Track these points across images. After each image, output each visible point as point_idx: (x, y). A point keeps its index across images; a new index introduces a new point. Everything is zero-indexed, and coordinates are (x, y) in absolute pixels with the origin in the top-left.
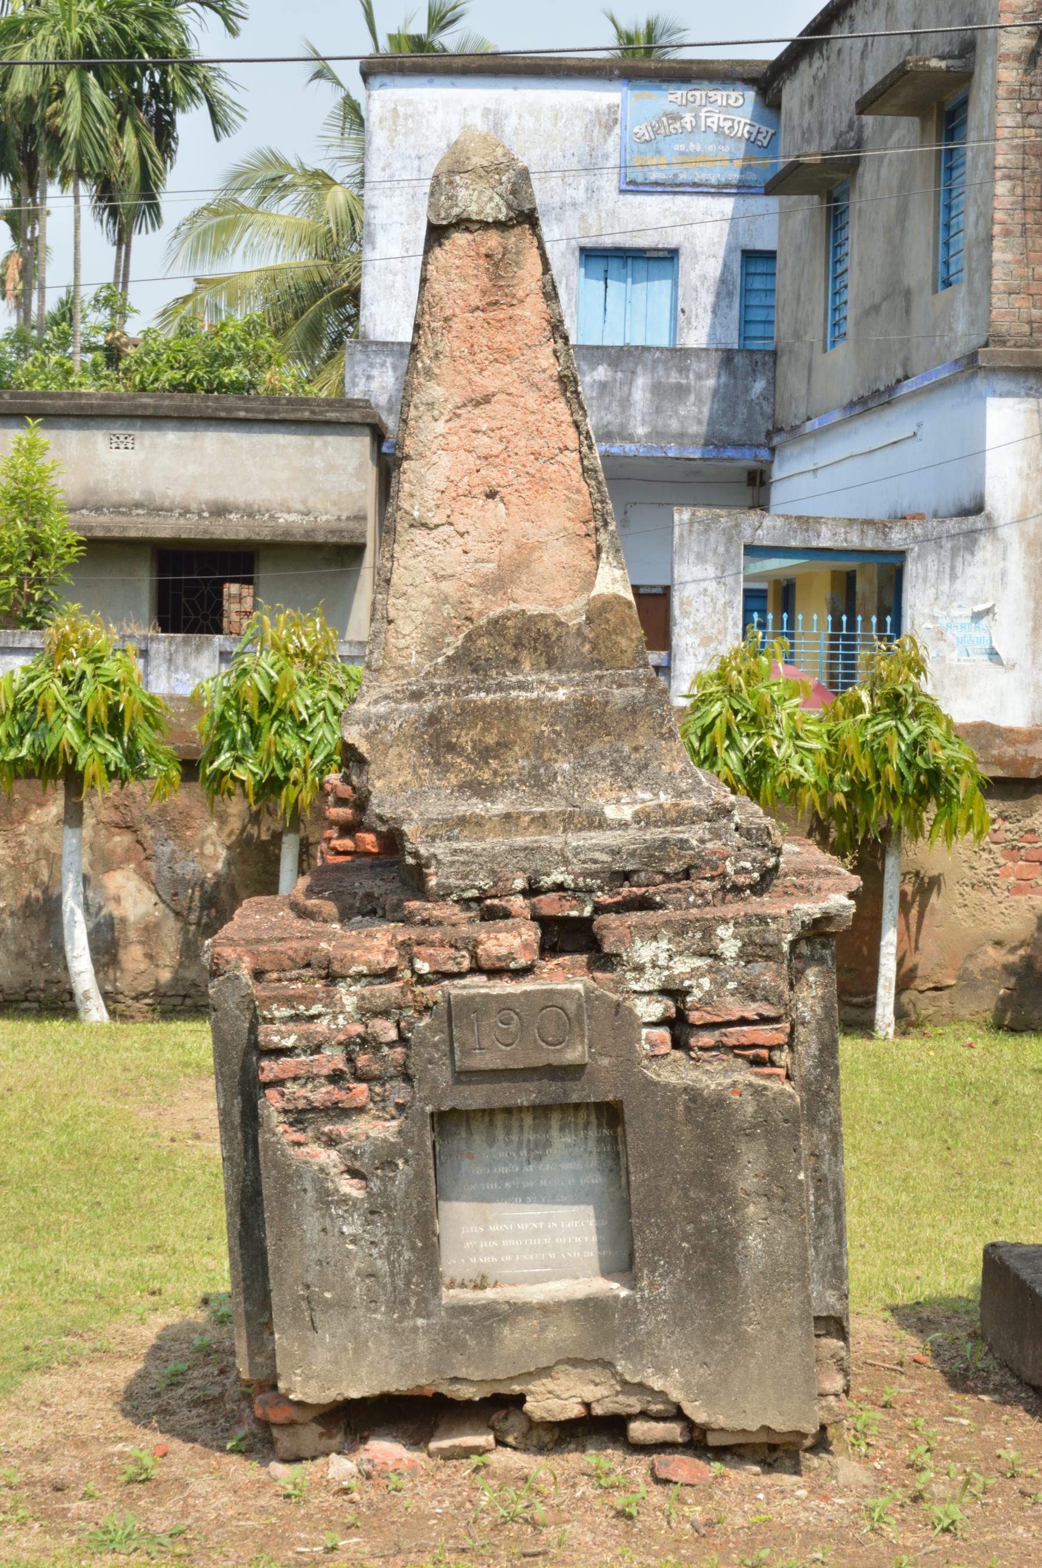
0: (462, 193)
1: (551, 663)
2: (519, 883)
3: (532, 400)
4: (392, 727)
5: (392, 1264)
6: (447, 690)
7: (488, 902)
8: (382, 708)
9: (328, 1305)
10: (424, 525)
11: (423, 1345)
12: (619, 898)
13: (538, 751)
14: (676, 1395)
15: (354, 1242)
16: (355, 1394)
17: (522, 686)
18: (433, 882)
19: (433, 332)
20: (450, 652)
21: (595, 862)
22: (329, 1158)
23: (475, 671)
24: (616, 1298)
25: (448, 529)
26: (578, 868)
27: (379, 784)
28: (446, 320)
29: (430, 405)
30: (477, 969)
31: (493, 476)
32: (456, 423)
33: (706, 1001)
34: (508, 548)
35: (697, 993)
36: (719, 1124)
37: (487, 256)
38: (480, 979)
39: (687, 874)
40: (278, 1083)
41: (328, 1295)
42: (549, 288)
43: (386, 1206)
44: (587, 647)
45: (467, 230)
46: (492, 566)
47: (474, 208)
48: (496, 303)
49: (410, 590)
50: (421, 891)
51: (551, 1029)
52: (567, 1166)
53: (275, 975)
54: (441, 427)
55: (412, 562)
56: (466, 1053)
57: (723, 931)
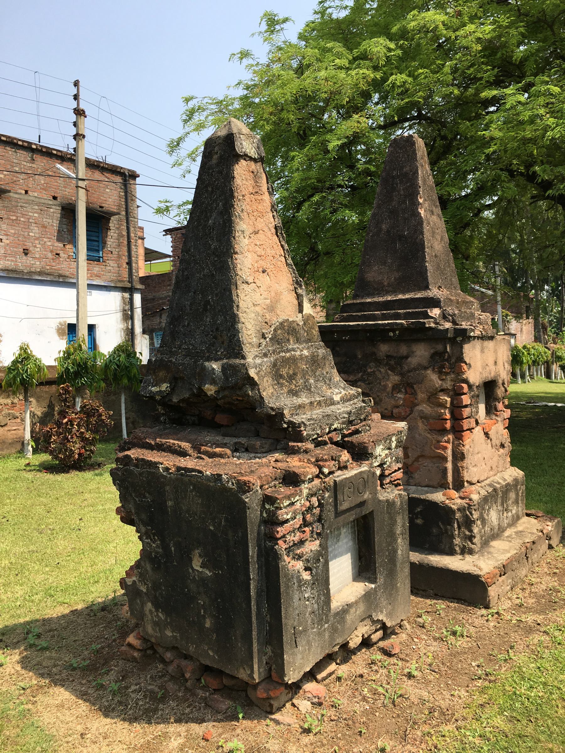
0: (244, 143)
1: (298, 341)
2: (327, 430)
3: (269, 234)
4: (264, 369)
5: (318, 604)
6: (274, 352)
7: (319, 439)
8: (258, 361)
9: (301, 632)
10: (247, 283)
11: (327, 635)
12: (350, 431)
13: (304, 376)
14: (385, 620)
15: (308, 600)
16: (308, 669)
17: (294, 350)
18: (305, 434)
19: (239, 200)
20: (270, 336)
21: (344, 418)
22: (299, 565)
23: (278, 344)
24: (372, 588)
25: (253, 284)
26: (340, 421)
27: (264, 394)
28: (243, 196)
29: (243, 232)
30: (340, 468)
31: (263, 264)
32: (251, 240)
33: (389, 466)
34: (273, 294)
35: (388, 463)
36: (393, 511)
37: (252, 172)
38: (339, 473)
39: (365, 419)
40: (284, 536)
41: (301, 628)
42: (271, 190)
43: (317, 580)
44: (306, 334)
45: (245, 159)
46: (269, 301)
47: (248, 150)
48: (257, 192)
49: (247, 310)
50: (301, 439)
51: (361, 488)
52: (345, 541)
53: (267, 486)
54: (246, 241)
55: (245, 298)
56: (341, 505)
57: (394, 439)
